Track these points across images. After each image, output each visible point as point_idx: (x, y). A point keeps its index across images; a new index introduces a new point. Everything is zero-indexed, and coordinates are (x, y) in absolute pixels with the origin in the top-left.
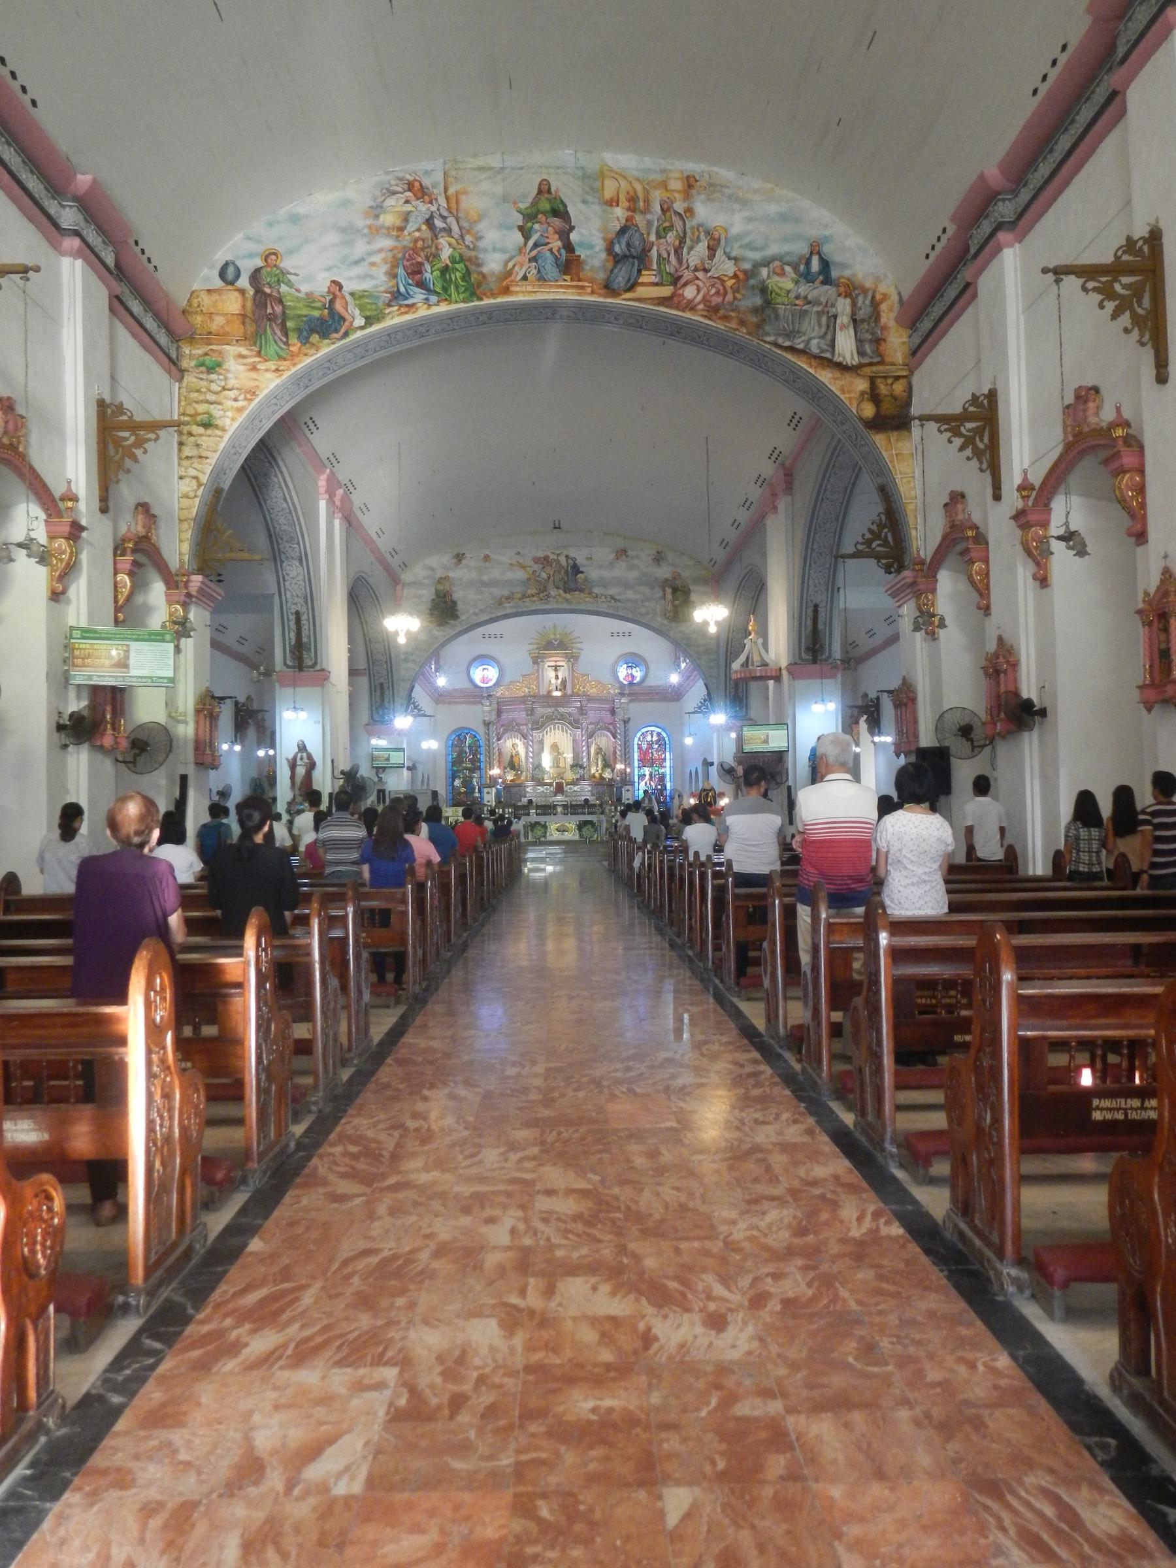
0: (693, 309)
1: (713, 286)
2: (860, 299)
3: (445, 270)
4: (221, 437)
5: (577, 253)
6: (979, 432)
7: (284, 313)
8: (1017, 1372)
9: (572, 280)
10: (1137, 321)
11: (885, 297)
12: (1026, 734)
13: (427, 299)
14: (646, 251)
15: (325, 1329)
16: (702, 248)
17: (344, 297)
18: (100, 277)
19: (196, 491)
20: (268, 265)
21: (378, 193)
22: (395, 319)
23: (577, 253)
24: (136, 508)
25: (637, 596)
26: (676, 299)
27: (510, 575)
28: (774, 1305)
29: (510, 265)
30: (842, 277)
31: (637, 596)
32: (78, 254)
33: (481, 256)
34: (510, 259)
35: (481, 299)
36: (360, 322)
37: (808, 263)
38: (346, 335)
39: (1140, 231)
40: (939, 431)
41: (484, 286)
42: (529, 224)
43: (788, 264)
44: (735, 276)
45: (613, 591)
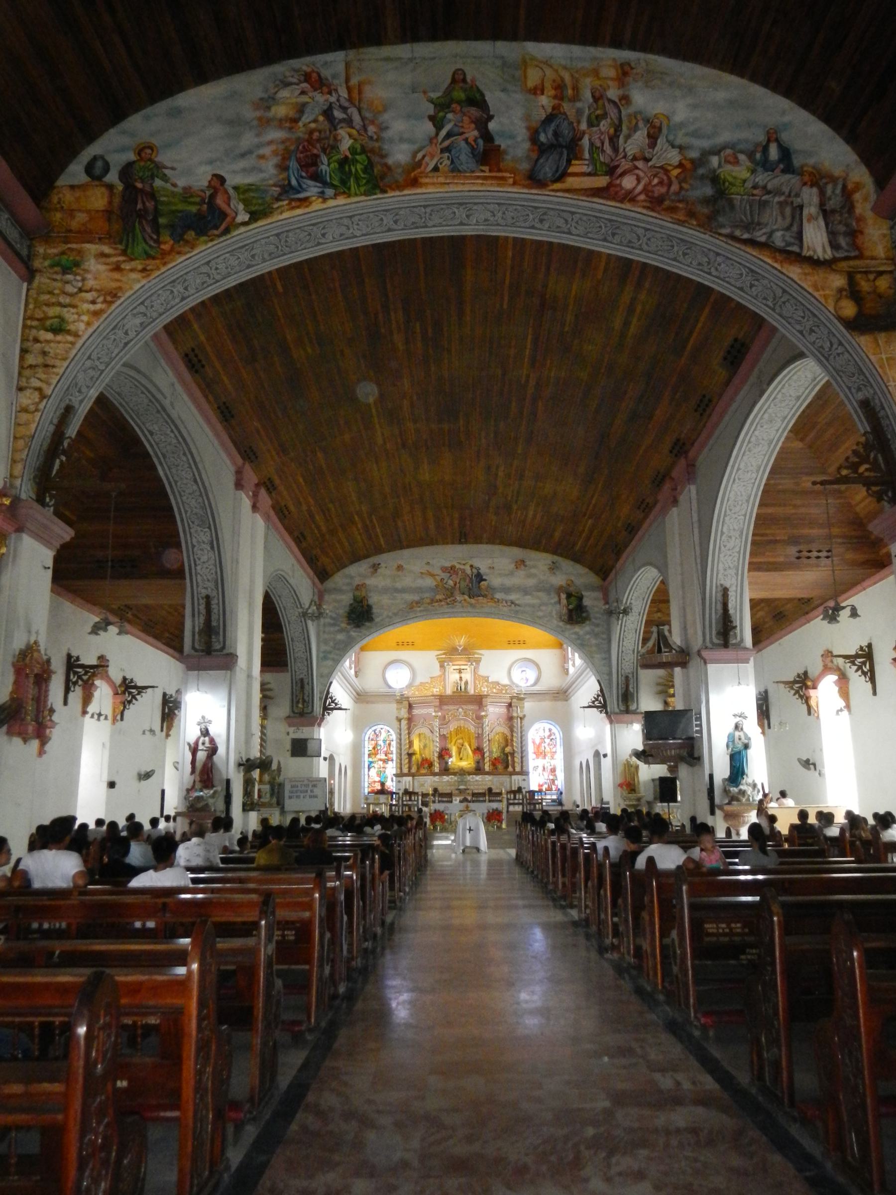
0: (633, 200)
1: (655, 176)
2: (829, 189)
3: (344, 162)
4: (73, 344)
5: (497, 143)
7: (156, 209)
9: (490, 171)
11: (858, 187)
13: (323, 193)
16: (640, 136)
17: (226, 192)
19: (37, 404)
20: (141, 159)
23: (497, 143)
25: (536, 601)
29: (419, 156)
30: (806, 165)
31: (536, 601)
33: (386, 147)
34: (420, 150)
36: (243, 217)
37: (765, 149)
38: (227, 231)
41: (386, 180)
42: (441, 114)
43: (742, 152)
44: (681, 165)
45: (513, 597)
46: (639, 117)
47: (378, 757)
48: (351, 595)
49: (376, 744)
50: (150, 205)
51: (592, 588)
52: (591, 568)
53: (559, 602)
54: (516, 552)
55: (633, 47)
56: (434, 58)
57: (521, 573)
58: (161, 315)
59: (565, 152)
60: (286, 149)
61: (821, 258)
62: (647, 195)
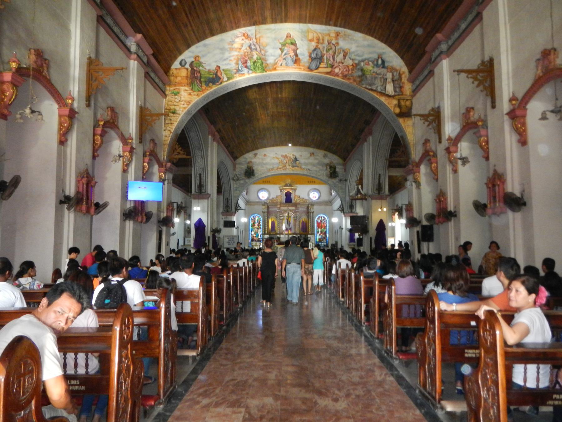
1: (345, 68)
2: (395, 74)
3: (255, 62)
5: (299, 57)
6: (434, 120)
8: (422, 415)
10: (485, 88)
11: (404, 73)
12: (450, 223)
15: (223, 399)
16: (341, 56)
17: (220, 71)
18: (142, 67)
24: (150, 141)
26: (332, 73)
27: (273, 161)
28: (353, 396)
29: (276, 61)
31: (318, 169)
32: (135, 60)
36: (226, 79)
37: (377, 60)
38: (221, 83)
39: (487, 58)
40: (421, 120)
41: (267, 68)
42: (283, 48)
43: (371, 61)
44: (353, 65)
45: (309, 167)
48: (246, 166)
49: (254, 222)
50: (199, 75)
51: (340, 165)
52: (339, 156)
54: (311, 150)
55: (340, 26)
57: (312, 158)
60: (238, 58)
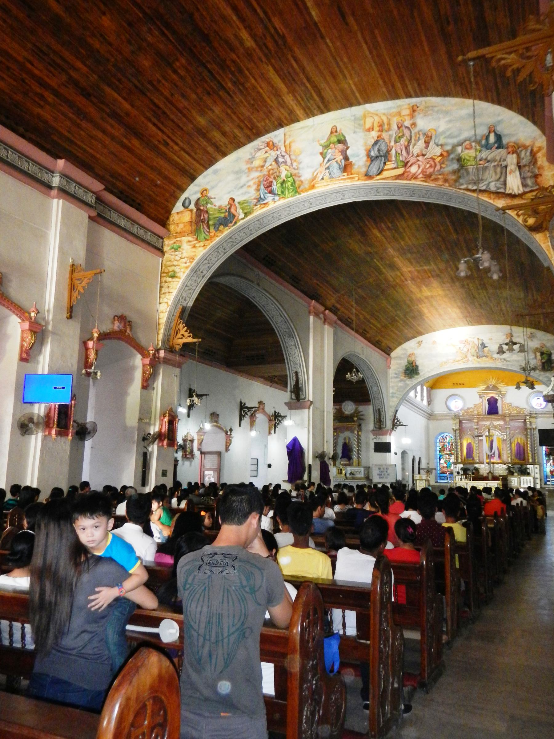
0: (416, 178)
1: (428, 163)
2: (523, 154)
5: (350, 160)
7: (208, 217)
9: (347, 175)
13: (274, 199)
14: (388, 152)
16: (421, 144)
17: (235, 205)
21: (253, 151)
22: (258, 212)
26: (406, 175)
29: (315, 174)
30: (511, 142)
32: (59, 197)
33: (300, 172)
35: (300, 194)
36: (242, 216)
37: (487, 138)
38: (235, 223)
41: (301, 189)
42: (326, 151)
44: (442, 155)
46: (420, 133)
47: (446, 452)
49: (444, 445)
50: (206, 216)
53: (536, 358)
55: (417, 96)
56: (322, 123)
58: (216, 262)
59: (383, 159)
60: (260, 182)
61: (517, 194)
62: (423, 174)
